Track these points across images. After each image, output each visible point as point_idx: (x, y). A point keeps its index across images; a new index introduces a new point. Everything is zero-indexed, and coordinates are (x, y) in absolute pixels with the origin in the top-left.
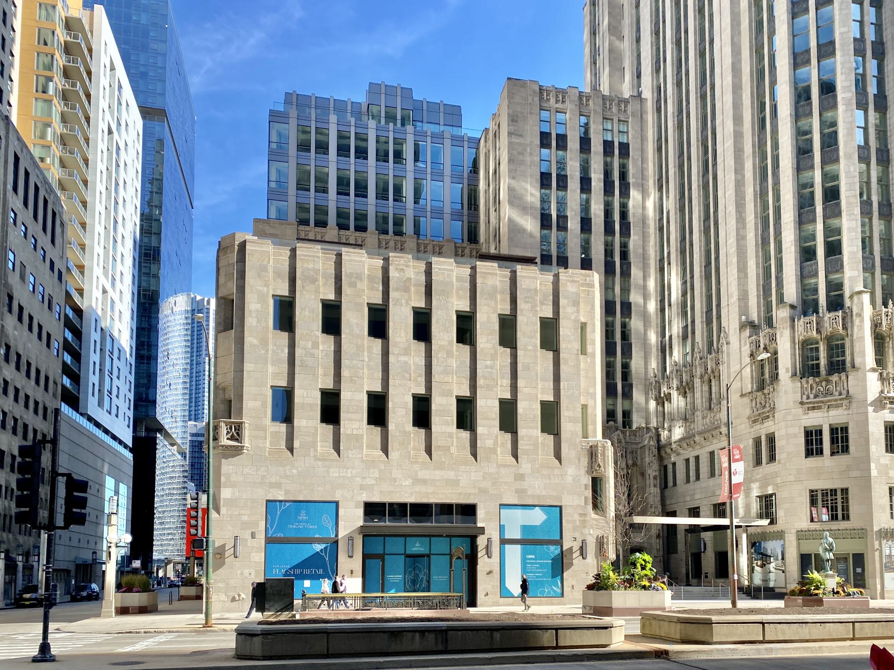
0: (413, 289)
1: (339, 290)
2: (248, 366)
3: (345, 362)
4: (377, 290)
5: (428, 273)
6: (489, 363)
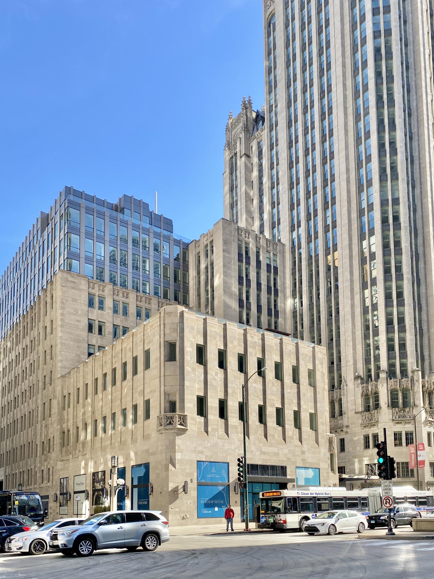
0: (257, 347)
1: (225, 345)
2: (187, 383)
3: (229, 385)
4: (242, 346)
5: (263, 339)
6: (289, 391)
